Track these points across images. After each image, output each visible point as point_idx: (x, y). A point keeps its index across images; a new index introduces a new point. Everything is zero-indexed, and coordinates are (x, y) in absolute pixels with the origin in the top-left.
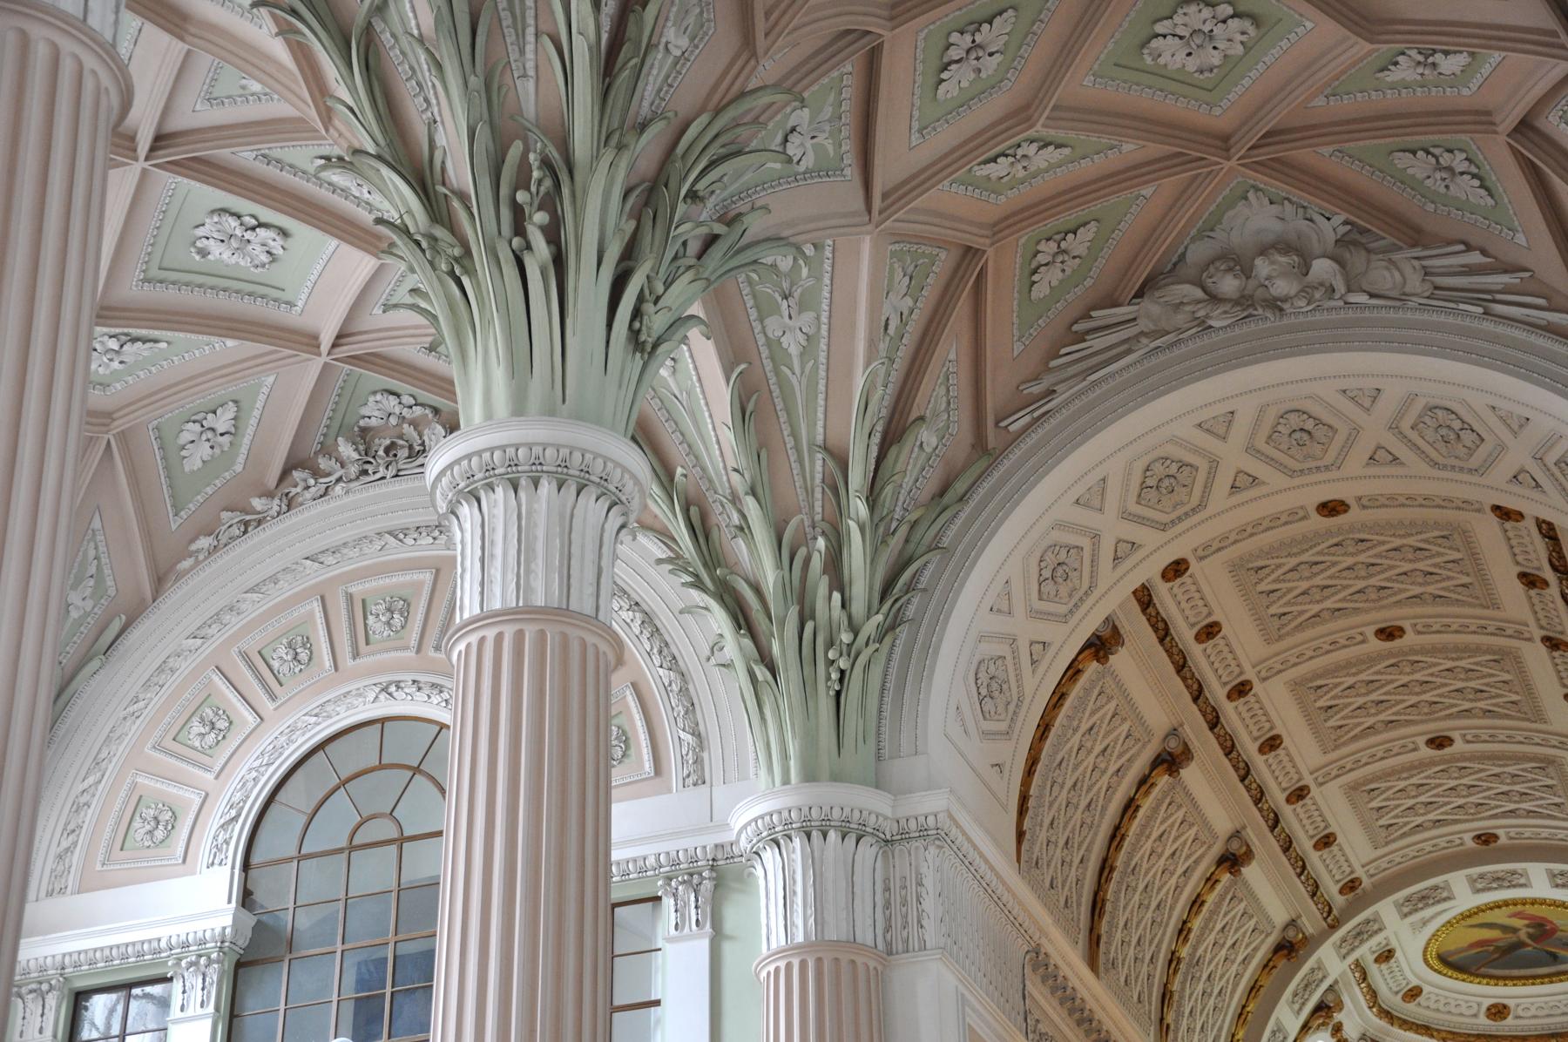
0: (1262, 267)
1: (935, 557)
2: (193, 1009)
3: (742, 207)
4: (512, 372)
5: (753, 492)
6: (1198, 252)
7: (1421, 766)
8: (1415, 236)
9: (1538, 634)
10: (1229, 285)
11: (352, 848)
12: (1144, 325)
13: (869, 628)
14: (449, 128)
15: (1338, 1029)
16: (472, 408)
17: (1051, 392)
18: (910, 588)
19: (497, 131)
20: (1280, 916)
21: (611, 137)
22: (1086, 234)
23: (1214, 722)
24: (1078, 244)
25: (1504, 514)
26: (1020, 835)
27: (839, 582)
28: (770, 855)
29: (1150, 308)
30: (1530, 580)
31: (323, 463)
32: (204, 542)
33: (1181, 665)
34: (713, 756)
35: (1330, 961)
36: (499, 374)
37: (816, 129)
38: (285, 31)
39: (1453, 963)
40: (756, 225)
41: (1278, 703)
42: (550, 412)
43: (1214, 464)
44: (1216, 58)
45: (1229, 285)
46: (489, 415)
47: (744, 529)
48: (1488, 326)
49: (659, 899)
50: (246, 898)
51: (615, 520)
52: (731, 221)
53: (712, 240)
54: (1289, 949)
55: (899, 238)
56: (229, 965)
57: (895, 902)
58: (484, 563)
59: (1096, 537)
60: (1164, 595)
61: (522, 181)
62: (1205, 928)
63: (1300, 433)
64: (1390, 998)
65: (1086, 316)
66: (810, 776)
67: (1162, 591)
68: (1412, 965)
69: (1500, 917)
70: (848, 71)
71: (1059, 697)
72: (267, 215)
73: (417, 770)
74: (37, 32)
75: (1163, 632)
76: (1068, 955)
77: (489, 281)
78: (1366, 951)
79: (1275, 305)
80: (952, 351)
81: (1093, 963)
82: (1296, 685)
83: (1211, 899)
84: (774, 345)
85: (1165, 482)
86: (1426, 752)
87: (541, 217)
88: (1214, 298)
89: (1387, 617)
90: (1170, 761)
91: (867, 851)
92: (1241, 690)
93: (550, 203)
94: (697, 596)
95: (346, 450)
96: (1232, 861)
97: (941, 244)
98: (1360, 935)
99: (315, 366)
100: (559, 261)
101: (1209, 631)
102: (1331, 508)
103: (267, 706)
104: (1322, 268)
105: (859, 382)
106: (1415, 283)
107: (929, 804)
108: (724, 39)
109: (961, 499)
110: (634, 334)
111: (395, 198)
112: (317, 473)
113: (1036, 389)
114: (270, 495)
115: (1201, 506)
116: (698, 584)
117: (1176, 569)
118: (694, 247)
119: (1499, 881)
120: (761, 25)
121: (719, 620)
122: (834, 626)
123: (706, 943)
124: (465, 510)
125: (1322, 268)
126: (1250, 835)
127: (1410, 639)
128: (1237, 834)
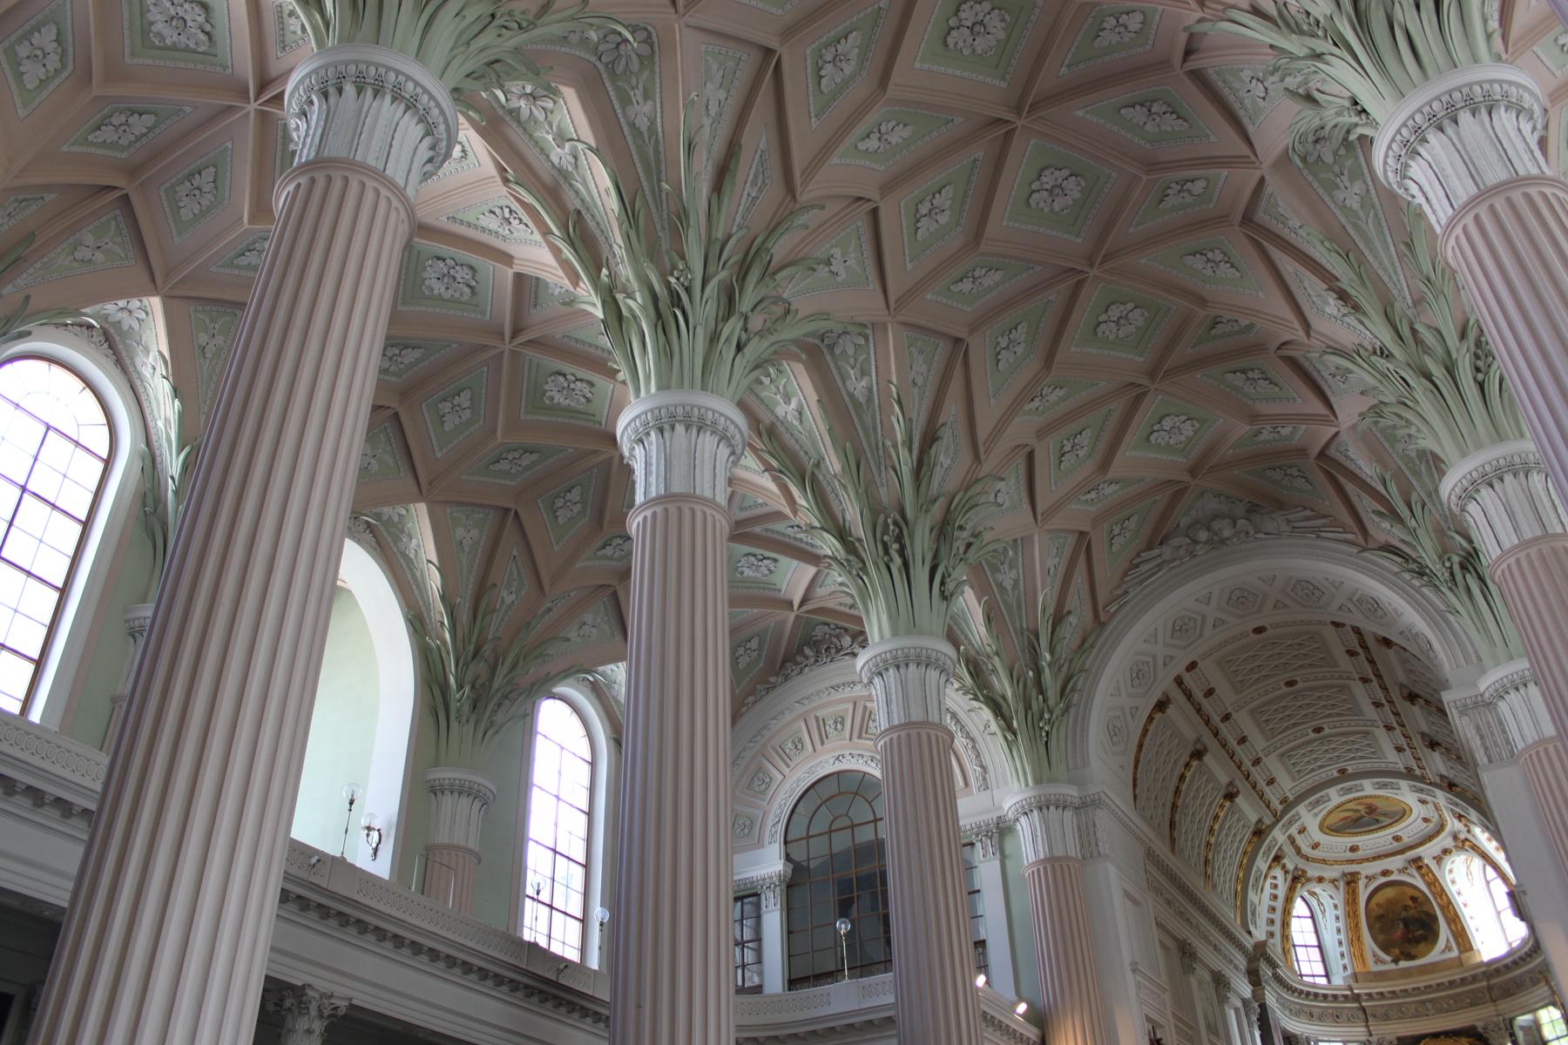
0: (1216, 525)
1: (1083, 675)
2: (771, 907)
3: (981, 528)
4: (890, 616)
5: (997, 654)
6: (1184, 522)
7: (1311, 742)
8: (1281, 505)
10: (1203, 535)
11: (831, 831)
12: (1166, 557)
13: (1057, 712)
14: (852, 512)
15: (1284, 867)
16: (873, 633)
17: (1126, 592)
18: (1073, 690)
19: (874, 510)
20: (1254, 818)
21: (923, 508)
22: (1135, 519)
23: (1216, 734)
24: (1131, 524)
25: (1336, 625)
26: (1135, 797)
27: (1041, 691)
28: (1023, 820)
29: (1167, 551)
30: (1351, 653)
31: (799, 659)
32: (751, 699)
33: (1199, 710)
34: (991, 775)
35: (1278, 836)
36: (884, 618)
37: (1010, 490)
38: (775, 479)
40: (987, 536)
41: (1244, 721)
42: (908, 633)
43: (1204, 617)
44: (1182, 438)
45: (1203, 535)
46: (882, 637)
47: (994, 671)
48: (1319, 542)
49: (972, 844)
50: (788, 858)
51: (943, 678)
52: (976, 535)
53: (969, 545)
54: (1259, 833)
55: (1050, 531)
56: (784, 886)
57: (1087, 835)
58: (883, 703)
59: (1154, 657)
60: (1188, 679)
61: (885, 531)
62: (1221, 829)
63: (1241, 599)
64: (1306, 850)
65: (1138, 555)
66: (1038, 781)
68: (1316, 834)
69: (1352, 806)
70: (1021, 462)
71: (1145, 731)
72: (767, 554)
73: (856, 794)
74: (698, 508)
75: (1189, 695)
76: (1162, 849)
77: (875, 576)
78: (1293, 830)
79: (1223, 541)
80: (1080, 577)
81: (1173, 851)
82: (1252, 712)
83: (1222, 814)
84: (1000, 585)
85: (1181, 629)
86: (1313, 735)
87: (896, 546)
88: (1195, 542)
89: (1289, 676)
90: (1198, 754)
91: (1068, 814)
92: (1227, 717)
93: (899, 539)
94: (975, 703)
95: (807, 651)
96: (1230, 796)
97: (1071, 531)
98: (1290, 823)
99: (792, 616)
100: (906, 565)
101: (1210, 693)
102: (1259, 630)
103: (786, 770)
104: (1241, 523)
105: (1041, 599)
106: (1284, 527)
107: (1092, 790)
108: (966, 457)
109: (1092, 647)
110: (942, 593)
111: (828, 545)
112: (796, 663)
113: (1119, 592)
114: (777, 675)
115: (1201, 635)
116: (976, 699)
117: (1192, 666)
118: (962, 550)
119: (1350, 790)
120: (982, 449)
121: (986, 714)
122: (1038, 712)
123: (997, 863)
124: (877, 680)
125: (1241, 523)
126: (1237, 782)
127: (1300, 685)
128: (1231, 783)
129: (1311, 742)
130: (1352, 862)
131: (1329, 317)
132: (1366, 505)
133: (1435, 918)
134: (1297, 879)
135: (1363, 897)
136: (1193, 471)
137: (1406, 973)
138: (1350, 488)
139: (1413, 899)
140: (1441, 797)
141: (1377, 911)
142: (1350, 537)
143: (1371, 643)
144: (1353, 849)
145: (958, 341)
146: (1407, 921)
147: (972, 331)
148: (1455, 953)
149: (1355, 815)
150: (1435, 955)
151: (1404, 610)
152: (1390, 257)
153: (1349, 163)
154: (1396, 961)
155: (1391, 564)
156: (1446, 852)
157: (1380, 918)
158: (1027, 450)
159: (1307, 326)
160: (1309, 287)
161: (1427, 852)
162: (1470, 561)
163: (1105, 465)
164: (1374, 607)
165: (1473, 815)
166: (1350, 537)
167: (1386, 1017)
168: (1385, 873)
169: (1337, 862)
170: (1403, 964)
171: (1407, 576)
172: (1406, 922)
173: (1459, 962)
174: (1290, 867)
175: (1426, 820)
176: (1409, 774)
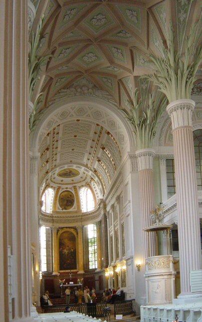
7: (69, 152)
8: (102, 89)
9: (92, 139)
24: (63, 80)
25: (98, 125)
30: (95, 133)
35: (50, 174)
39: (60, 175)
45: (79, 90)
54: (47, 172)
64: (52, 179)
67: (57, 128)
68: (56, 176)
69: (67, 170)
85: (63, 115)
90: (47, 149)
102: (78, 120)
104: (90, 90)
117: (59, 125)
125: (90, 90)
129: (69, 152)
130: (60, 184)
131: (157, 46)
132: (124, 98)
133: (74, 201)
134: (47, 186)
135: (60, 192)
136: (86, 71)
137: (64, 213)
138: (122, 91)
139: (71, 195)
140: (90, 173)
141: (62, 197)
142: (116, 104)
143: (103, 131)
144: (62, 181)
145: (59, 6)
146: (67, 200)
147: (64, 5)
148: (76, 210)
149: (66, 172)
150: (71, 210)
151: (122, 128)
152: (182, 39)
153: (186, 7)
154: (62, 209)
155: (124, 115)
156: (83, 186)
157: (62, 199)
158: (55, 49)
159: (148, 45)
160: (155, 34)
161: (79, 185)
162: (145, 121)
163: (68, 61)
164: (113, 124)
165: (96, 179)
166: (116, 104)
167: (57, 222)
168: (67, 188)
169: (57, 183)
170: (64, 210)
171: (127, 119)
172: (67, 201)
173: (76, 212)
174: (47, 182)
175: (81, 178)
176: (86, 166)
